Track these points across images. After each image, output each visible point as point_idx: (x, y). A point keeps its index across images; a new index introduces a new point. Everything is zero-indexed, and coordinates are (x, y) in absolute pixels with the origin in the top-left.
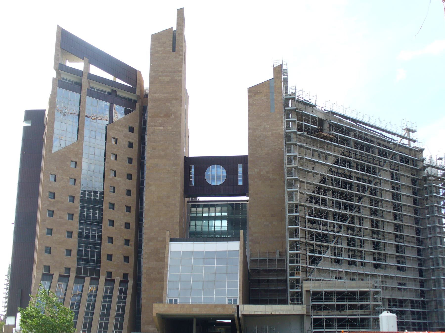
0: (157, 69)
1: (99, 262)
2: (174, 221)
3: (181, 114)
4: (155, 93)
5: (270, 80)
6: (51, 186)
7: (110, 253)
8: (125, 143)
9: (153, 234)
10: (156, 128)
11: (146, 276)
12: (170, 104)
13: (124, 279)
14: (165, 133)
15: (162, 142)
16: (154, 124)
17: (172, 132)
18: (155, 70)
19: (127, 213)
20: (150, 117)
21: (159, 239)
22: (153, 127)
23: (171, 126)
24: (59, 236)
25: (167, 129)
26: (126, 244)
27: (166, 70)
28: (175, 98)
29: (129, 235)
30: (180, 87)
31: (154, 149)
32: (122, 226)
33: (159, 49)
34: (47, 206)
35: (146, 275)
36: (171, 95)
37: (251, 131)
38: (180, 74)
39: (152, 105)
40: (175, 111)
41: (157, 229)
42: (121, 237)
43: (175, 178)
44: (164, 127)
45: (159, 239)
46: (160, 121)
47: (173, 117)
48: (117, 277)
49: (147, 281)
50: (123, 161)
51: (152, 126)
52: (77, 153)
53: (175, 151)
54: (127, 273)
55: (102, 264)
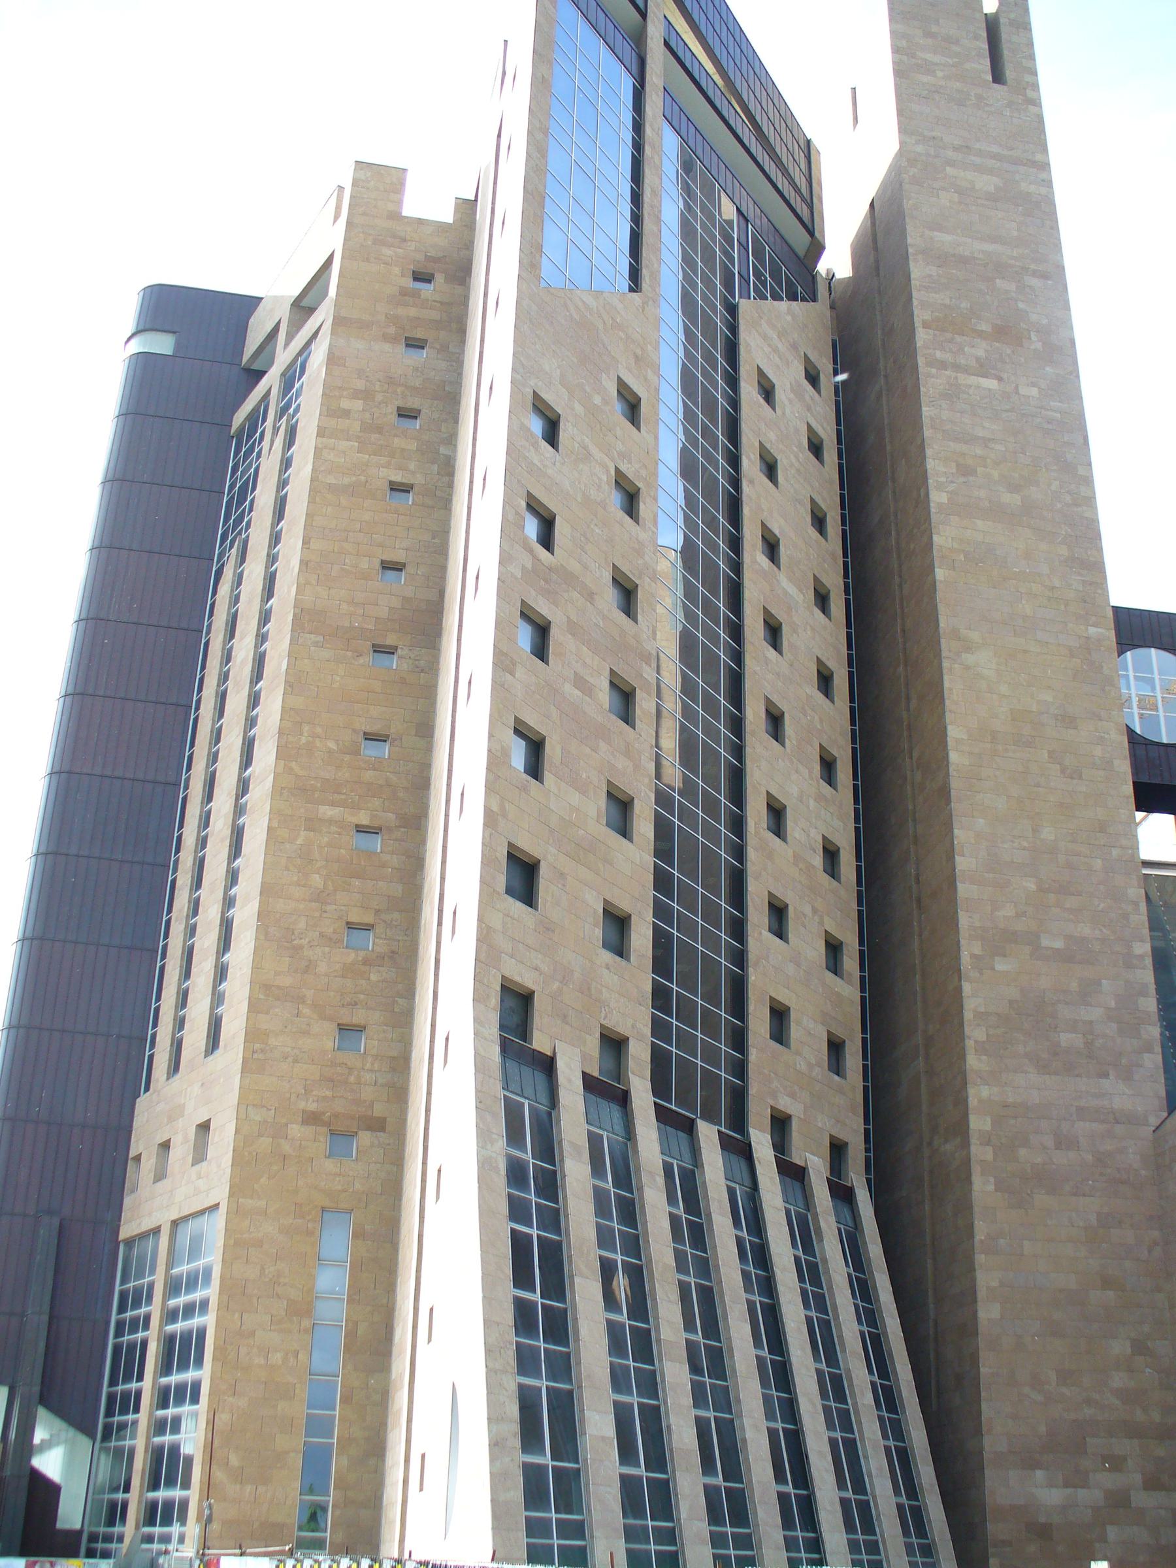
0: (934, 134)
1: (739, 1040)
2: (1115, 853)
6: (536, 462)
7: (784, 996)
8: (798, 422)
9: (1008, 911)
10: (959, 374)
11: (989, 1156)
12: (1013, 287)
13: (831, 1175)
14: (1007, 411)
15: (1001, 448)
16: (948, 357)
19: (826, 789)
20: (926, 325)
21: (1045, 942)
23: (1034, 385)
24: (575, 798)
25: (1017, 393)
26: (828, 968)
27: (978, 146)
28: (1033, 266)
30: (1052, 228)
31: (966, 471)
33: (929, 56)
34: (519, 577)
35: (989, 1149)
38: (1044, 176)
39: (930, 276)
40: (1045, 321)
41: (1031, 885)
43: (1092, 630)
44: (1000, 379)
45: (1045, 942)
46: (980, 349)
47: (1039, 346)
48: (814, 1155)
49: (996, 1190)
50: (798, 506)
51: (943, 365)
52: (639, 352)
53: (1068, 498)
54: (843, 1135)
55: (753, 1055)
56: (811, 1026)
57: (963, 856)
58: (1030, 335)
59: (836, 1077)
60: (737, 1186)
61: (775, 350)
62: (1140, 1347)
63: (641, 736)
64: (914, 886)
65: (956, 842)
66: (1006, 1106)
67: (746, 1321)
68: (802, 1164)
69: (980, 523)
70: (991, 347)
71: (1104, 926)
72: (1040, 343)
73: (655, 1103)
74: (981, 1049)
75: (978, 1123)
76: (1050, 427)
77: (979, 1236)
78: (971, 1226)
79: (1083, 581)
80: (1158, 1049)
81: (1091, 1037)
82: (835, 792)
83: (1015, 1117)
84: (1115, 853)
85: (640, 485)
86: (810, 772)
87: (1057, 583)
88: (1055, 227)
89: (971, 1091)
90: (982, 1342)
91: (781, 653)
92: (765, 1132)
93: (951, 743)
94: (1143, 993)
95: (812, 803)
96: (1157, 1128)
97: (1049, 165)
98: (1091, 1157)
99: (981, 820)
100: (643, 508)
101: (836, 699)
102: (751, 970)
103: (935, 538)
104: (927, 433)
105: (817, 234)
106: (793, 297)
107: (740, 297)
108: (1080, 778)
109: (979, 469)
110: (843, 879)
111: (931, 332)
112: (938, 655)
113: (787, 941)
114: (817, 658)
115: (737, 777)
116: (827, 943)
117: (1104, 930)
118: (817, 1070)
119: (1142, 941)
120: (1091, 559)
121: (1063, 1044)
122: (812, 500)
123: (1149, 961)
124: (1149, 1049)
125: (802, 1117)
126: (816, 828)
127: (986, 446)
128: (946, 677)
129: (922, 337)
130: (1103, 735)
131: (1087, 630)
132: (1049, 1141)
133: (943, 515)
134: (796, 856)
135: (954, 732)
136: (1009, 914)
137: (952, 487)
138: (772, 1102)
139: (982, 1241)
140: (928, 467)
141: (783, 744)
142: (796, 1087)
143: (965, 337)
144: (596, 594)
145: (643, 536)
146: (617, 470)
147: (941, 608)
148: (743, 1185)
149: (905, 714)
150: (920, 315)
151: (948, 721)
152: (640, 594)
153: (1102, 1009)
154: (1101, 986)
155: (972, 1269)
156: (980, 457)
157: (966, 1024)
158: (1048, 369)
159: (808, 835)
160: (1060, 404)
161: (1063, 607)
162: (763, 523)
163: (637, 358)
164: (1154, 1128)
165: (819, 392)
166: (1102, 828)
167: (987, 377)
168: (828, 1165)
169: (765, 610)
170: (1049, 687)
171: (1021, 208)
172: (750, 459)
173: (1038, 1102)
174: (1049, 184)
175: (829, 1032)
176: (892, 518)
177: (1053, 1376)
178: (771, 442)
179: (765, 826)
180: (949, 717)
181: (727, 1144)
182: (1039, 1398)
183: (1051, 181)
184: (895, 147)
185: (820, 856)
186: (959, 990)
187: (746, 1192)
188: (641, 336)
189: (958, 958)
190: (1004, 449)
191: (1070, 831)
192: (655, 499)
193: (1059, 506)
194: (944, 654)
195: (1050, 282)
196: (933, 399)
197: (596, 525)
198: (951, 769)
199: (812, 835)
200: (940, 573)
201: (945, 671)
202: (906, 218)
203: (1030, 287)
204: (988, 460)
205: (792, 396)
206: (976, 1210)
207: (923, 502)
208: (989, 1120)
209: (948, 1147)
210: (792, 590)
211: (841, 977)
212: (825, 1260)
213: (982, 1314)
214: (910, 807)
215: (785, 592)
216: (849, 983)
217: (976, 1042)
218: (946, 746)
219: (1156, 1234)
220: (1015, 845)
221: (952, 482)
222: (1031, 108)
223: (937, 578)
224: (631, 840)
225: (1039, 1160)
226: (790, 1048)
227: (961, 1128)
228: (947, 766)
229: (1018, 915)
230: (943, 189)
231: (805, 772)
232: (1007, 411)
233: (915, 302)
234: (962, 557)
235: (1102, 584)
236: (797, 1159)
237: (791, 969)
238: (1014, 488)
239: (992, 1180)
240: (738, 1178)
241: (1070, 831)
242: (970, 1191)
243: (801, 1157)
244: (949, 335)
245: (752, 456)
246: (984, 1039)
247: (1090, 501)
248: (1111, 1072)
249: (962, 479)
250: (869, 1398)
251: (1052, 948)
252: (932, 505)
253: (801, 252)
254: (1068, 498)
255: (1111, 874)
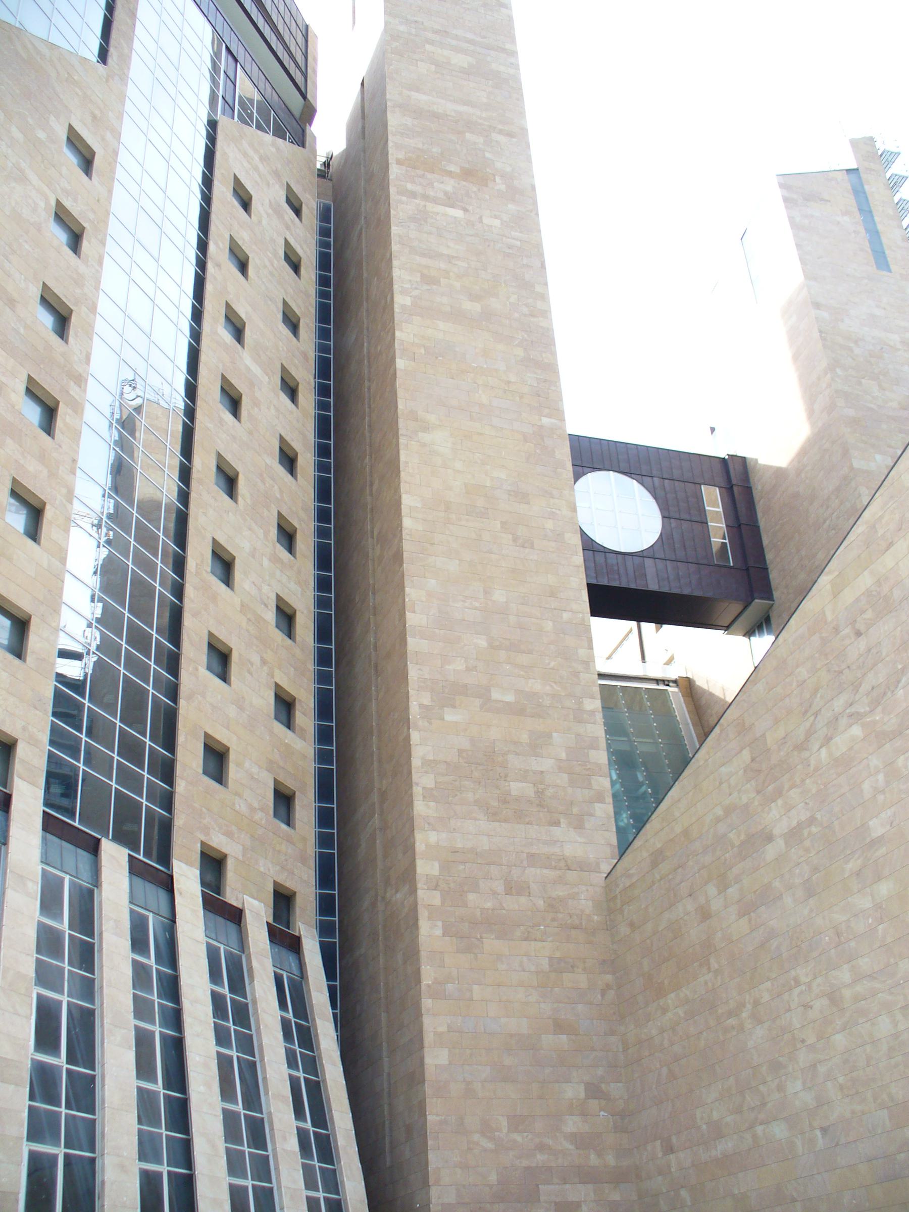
1: (167, 771)
2: (566, 616)
3: (533, 188)
4: (418, 90)
5: (848, 171)
7: (222, 735)
9: (459, 665)
10: (427, 203)
12: (481, 140)
13: (274, 921)
14: (471, 236)
16: (418, 189)
17: (504, 239)
18: (409, 17)
20: (399, 162)
21: (496, 695)
22: (415, 198)
23: (496, 217)
25: (481, 221)
26: (277, 718)
27: (454, 32)
28: (500, 127)
29: (293, 669)
30: (518, 99)
31: (429, 280)
32: (266, 605)
35: (437, 894)
36: (484, 115)
37: (825, 315)
40: (508, 169)
41: (482, 642)
42: (265, 668)
43: (545, 421)
44: (466, 210)
46: (449, 185)
48: (255, 899)
50: (270, 303)
51: (413, 195)
53: (525, 310)
54: (290, 884)
55: (181, 786)
56: (255, 770)
57: (414, 612)
58: (495, 179)
59: (284, 827)
60: (151, 916)
61: (256, 169)
62: (594, 1091)
63: (60, 446)
64: (373, 653)
65: (407, 600)
66: (455, 852)
67: (130, 1048)
68: (240, 906)
69: (441, 325)
70: (459, 184)
71: (555, 683)
72: (504, 186)
73: (44, 812)
74: (429, 795)
75: (425, 868)
76: (508, 251)
77: (427, 978)
78: (418, 973)
79: (537, 378)
80: (609, 799)
81: (543, 786)
82: (293, 558)
83: (464, 863)
84: (566, 616)
85: (85, 225)
86: (266, 534)
87: (513, 378)
88: (520, 98)
89: (419, 836)
90: (428, 1090)
91: (239, 421)
92: (192, 866)
93: (404, 510)
94: (594, 746)
95: (266, 562)
96: (609, 874)
97: (517, 53)
98: (542, 902)
99: (433, 581)
100: (85, 245)
101: (299, 476)
102: (182, 702)
103: (397, 334)
104: (395, 247)
105: (309, 96)
106: (279, 133)
107: (224, 113)
108: (532, 547)
109: (442, 280)
110: (298, 638)
111: (404, 168)
112: (396, 435)
113: (229, 684)
114: (281, 436)
115: (182, 521)
116: (277, 697)
117: (553, 684)
118: (259, 816)
119: (593, 697)
120: (546, 361)
121: (514, 793)
122: (285, 303)
123: (599, 717)
124: (600, 799)
125: (241, 858)
126: (269, 585)
127: (450, 262)
128: (402, 452)
129: (394, 171)
130: (554, 510)
131: (541, 420)
132: (499, 887)
133: (406, 315)
134: (244, 608)
135: (407, 501)
136: (458, 668)
137: (415, 293)
138: (203, 838)
139: (429, 986)
140: (394, 275)
141: (236, 502)
142: (234, 828)
143: (434, 175)
144: (18, 302)
145: (82, 268)
146: (58, 203)
147: (400, 393)
148: (158, 914)
149: (369, 498)
150: (394, 154)
151: (402, 490)
152: (74, 319)
153: (553, 760)
154: (549, 736)
155: (418, 1015)
156: (444, 270)
157: (413, 771)
158: (511, 206)
159: (260, 589)
160: (521, 234)
161: (518, 398)
162: (228, 305)
163: (94, 117)
164: (606, 875)
165: (301, 220)
166: (553, 594)
167: (453, 207)
168: (271, 911)
169: (224, 377)
170: (503, 466)
171: (491, 82)
172: (217, 244)
173: (487, 848)
174: (517, 67)
175: (276, 781)
176: (365, 331)
177: (504, 1123)
178: (244, 240)
179: (209, 569)
180: (403, 487)
181: (136, 869)
182: (490, 1146)
183: (518, 65)
184: (382, 26)
185: (272, 612)
186: (408, 738)
187: (162, 922)
188: (102, 101)
189: (407, 708)
190: (467, 266)
191: (522, 595)
192: (103, 243)
193: (516, 315)
194: (400, 432)
195: (514, 140)
196: (401, 221)
197: (26, 242)
198: (404, 533)
199: (263, 591)
200: (400, 363)
201: (401, 447)
202: (387, 80)
203: (497, 141)
204: (451, 274)
205: (270, 211)
206: (423, 954)
207: (388, 307)
208: (436, 865)
209: (399, 896)
210: (256, 370)
211: (294, 731)
212: (255, 1002)
213: (429, 1061)
214: (371, 582)
215: (248, 369)
216: (303, 737)
217: (423, 788)
218: (400, 514)
219: (609, 978)
220: (466, 604)
221: (416, 289)
222: (503, 10)
223: (398, 366)
224: (39, 544)
225: (489, 905)
226: (226, 786)
227: (409, 876)
228: (401, 530)
229: (468, 669)
230: (422, 61)
231: (261, 533)
232: (471, 236)
233: (390, 144)
234: (423, 351)
235: (556, 382)
236: (232, 896)
237: (232, 711)
238: (474, 297)
239: (440, 924)
240: (153, 905)
241: (522, 595)
242: (417, 936)
243: (237, 899)
244: (420, 172)
245: (221, 245)
246: (433, 786)
247: (545, 313)
248: (562, 820)
249: (426, 287)
250: (293, 1144)
251: (502, 701)
252: (396, 306)
253: (297, 114)
254: (525, 310)
255: (562, 635)
